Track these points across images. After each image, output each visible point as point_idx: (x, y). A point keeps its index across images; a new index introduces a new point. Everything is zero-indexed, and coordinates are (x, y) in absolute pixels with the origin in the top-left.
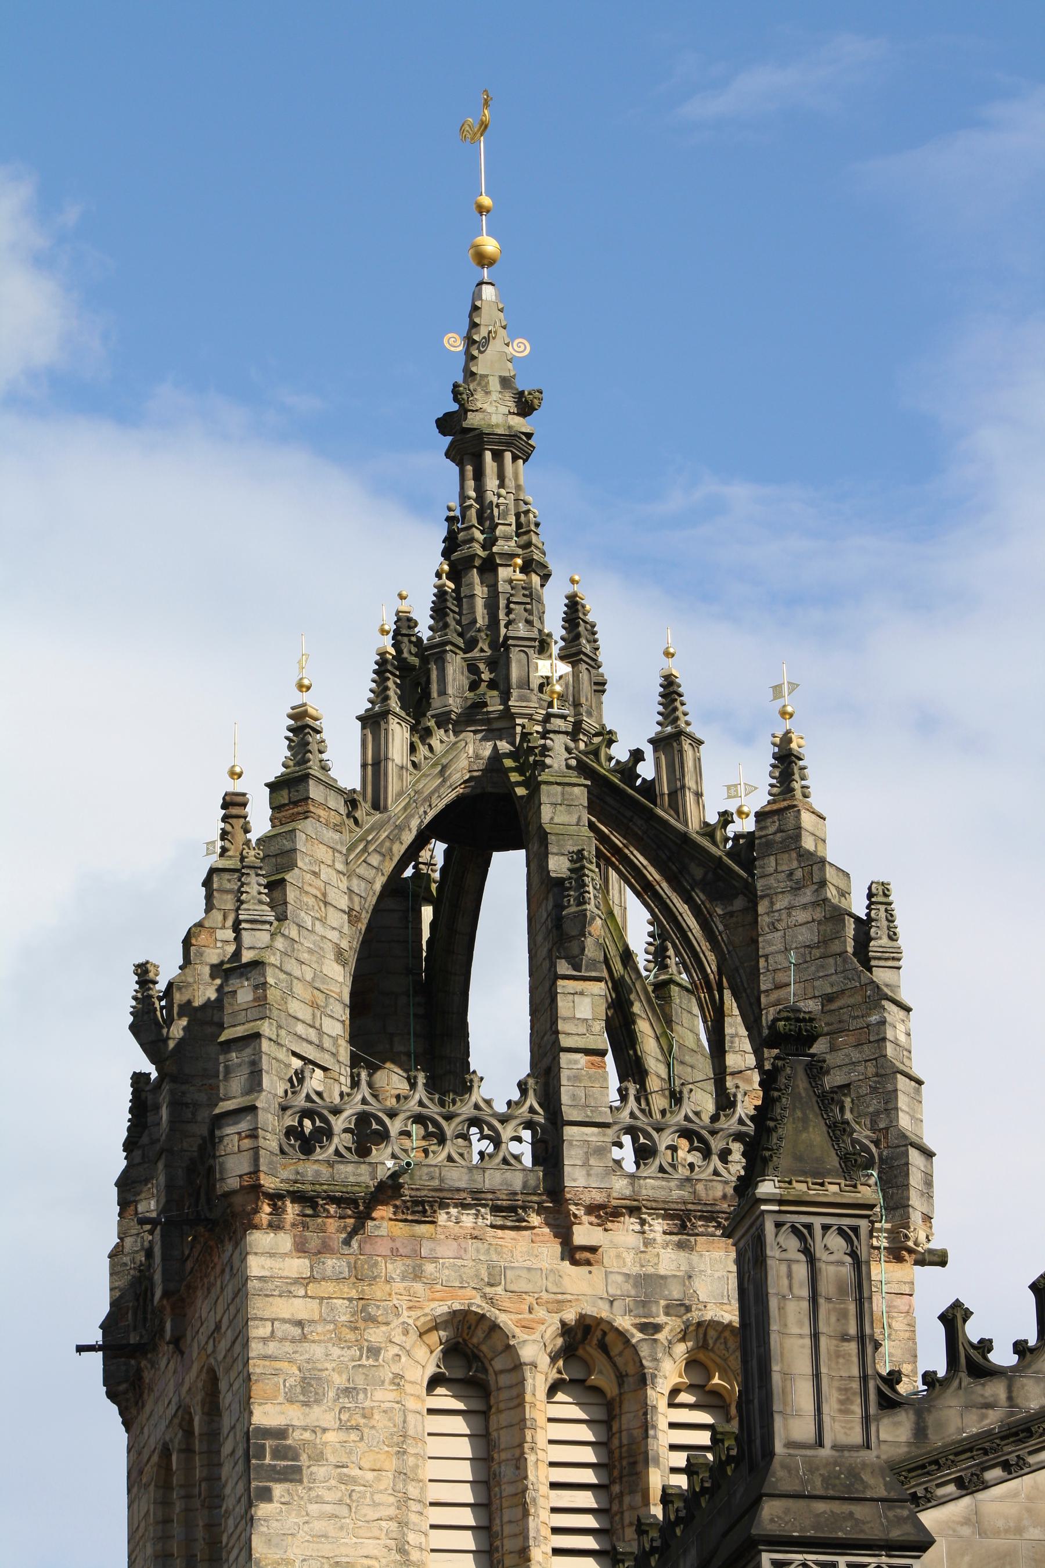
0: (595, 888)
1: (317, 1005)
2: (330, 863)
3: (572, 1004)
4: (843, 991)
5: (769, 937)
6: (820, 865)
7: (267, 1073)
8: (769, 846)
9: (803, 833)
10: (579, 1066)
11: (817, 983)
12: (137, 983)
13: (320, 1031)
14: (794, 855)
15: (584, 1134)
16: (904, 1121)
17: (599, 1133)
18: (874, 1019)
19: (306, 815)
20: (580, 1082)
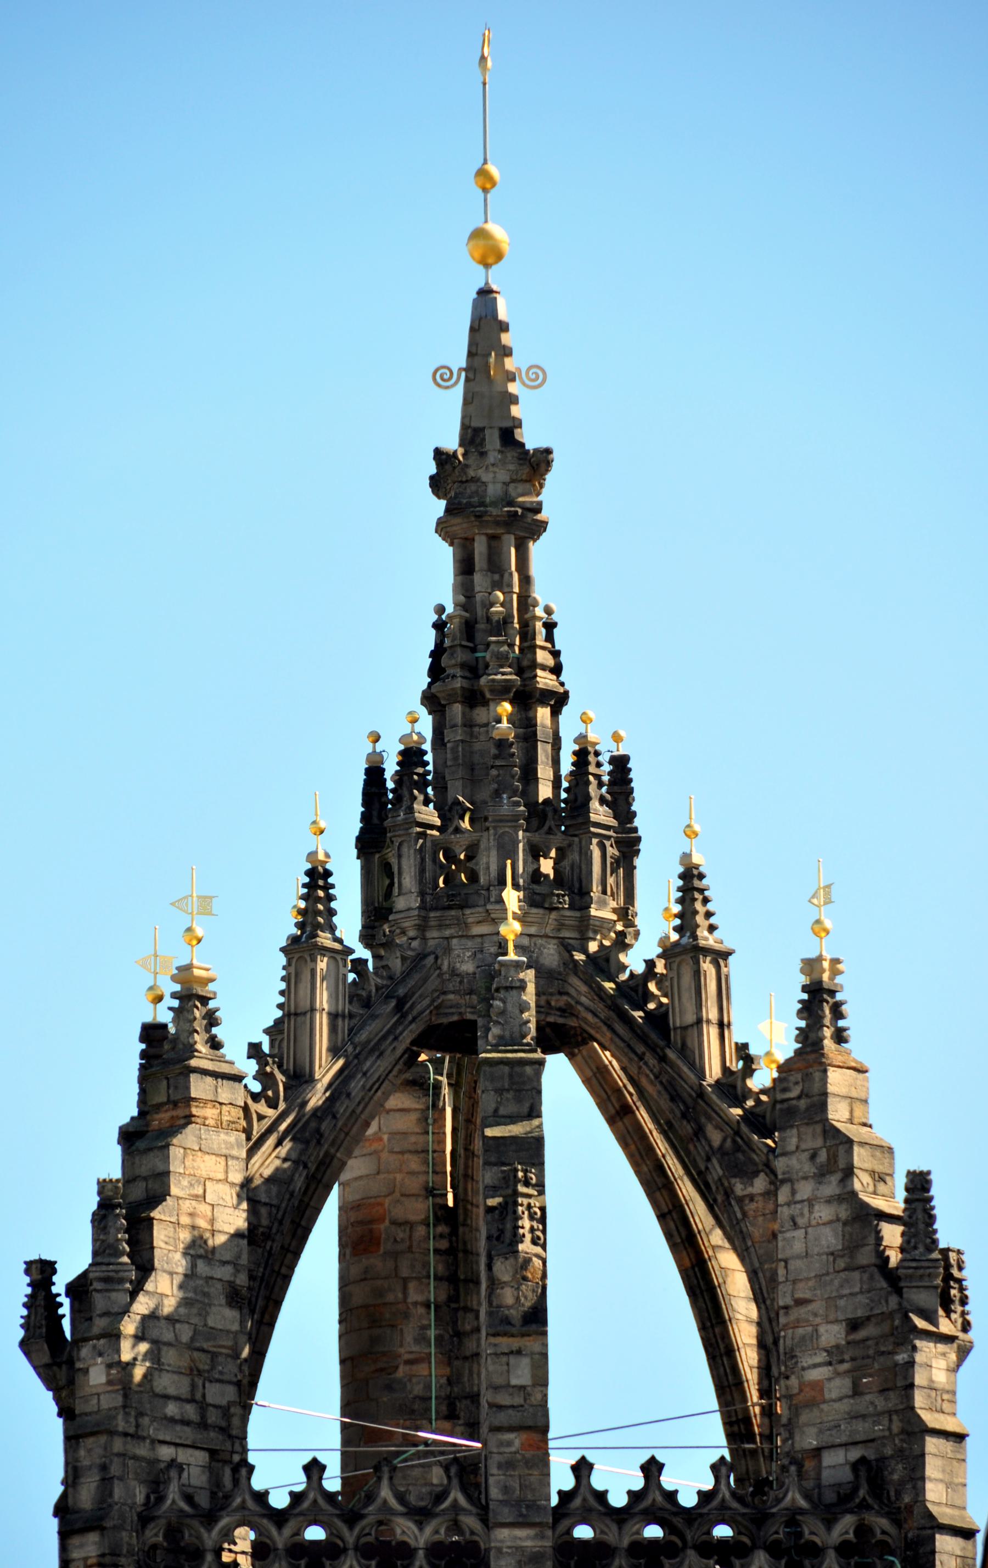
0: (532, 1217)
1: (198, 1370)
2: (221, 1176)
3: (505, 1367)
4: (868, 1318)
5: (788, 1235)
6: (847, 1146)
7: (121, 1479)
8: (791, 1112)
9: (830, 1100)
10: (513, 1449)
11: (842, 1303)
12: (29, 1285)
13: (203, 1406)
14: (819, 1128)
15: (516, 1538)
16: (934, 1493)
17: (536, 1535)
18: (901, 1358)
19: (189, 1119)
20: (514, 1469)
